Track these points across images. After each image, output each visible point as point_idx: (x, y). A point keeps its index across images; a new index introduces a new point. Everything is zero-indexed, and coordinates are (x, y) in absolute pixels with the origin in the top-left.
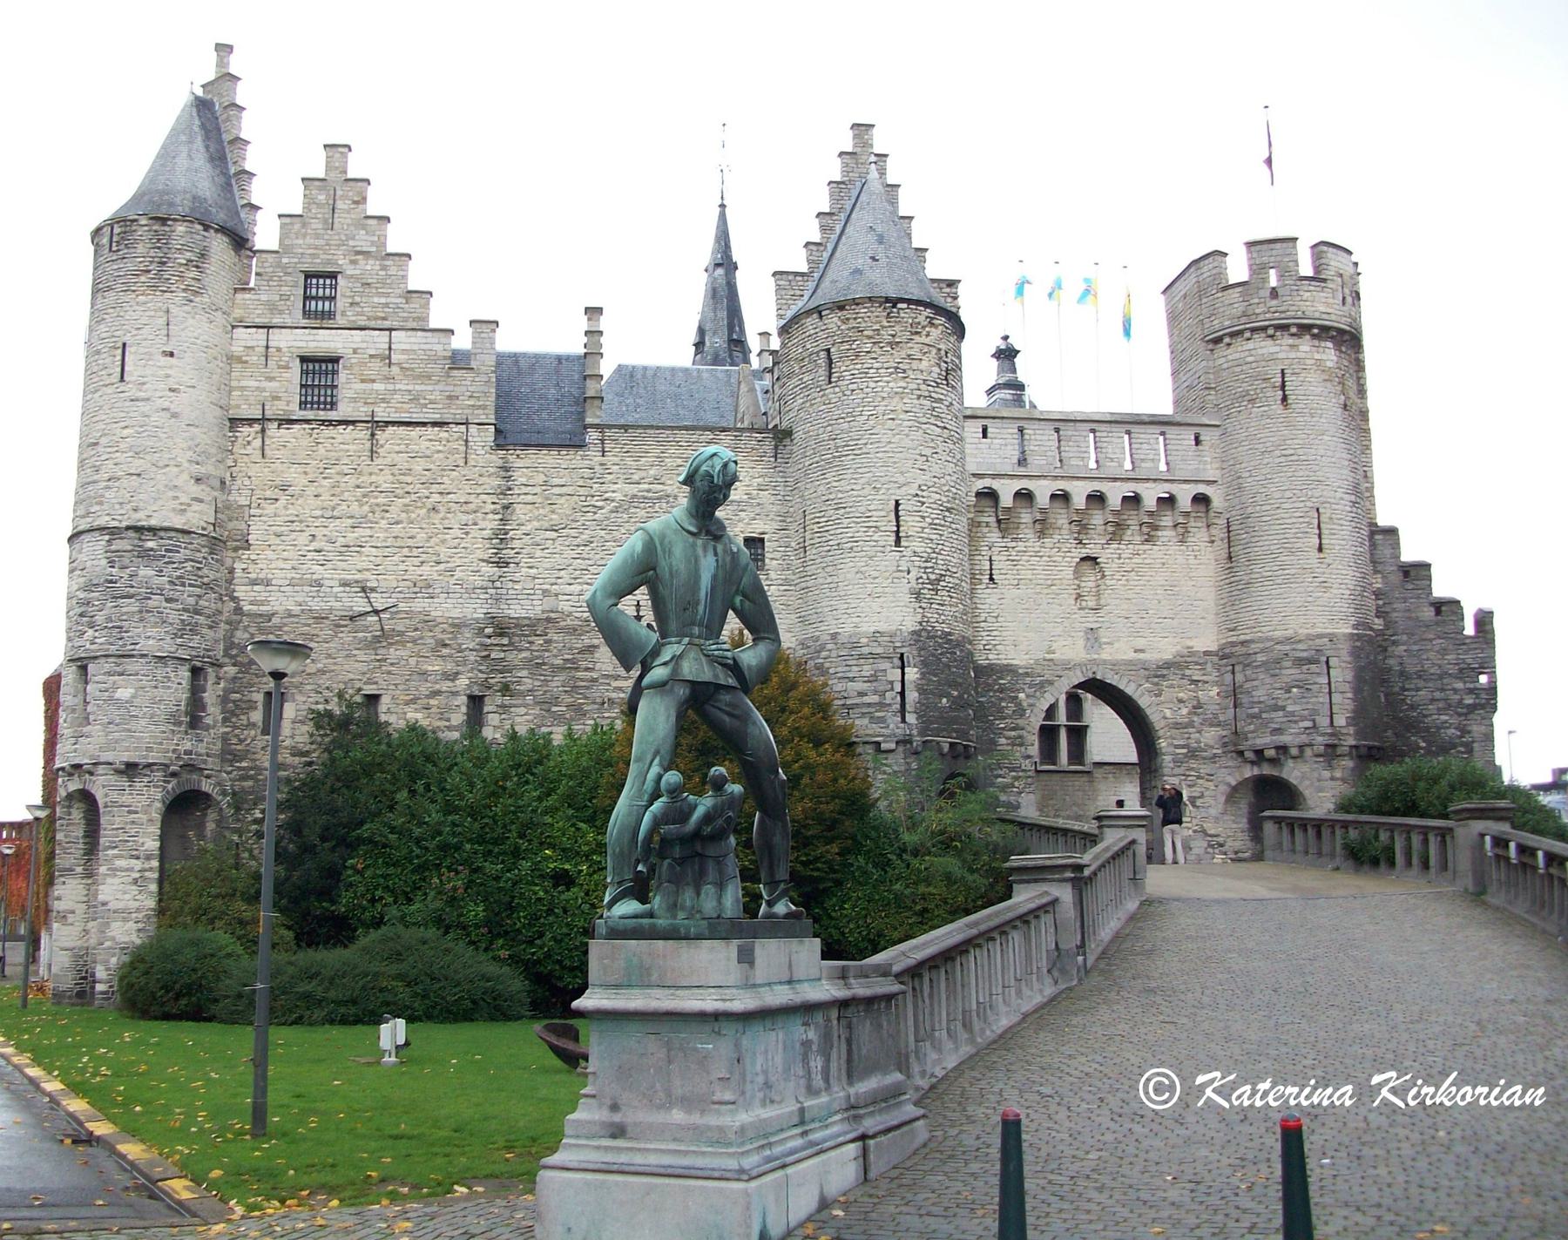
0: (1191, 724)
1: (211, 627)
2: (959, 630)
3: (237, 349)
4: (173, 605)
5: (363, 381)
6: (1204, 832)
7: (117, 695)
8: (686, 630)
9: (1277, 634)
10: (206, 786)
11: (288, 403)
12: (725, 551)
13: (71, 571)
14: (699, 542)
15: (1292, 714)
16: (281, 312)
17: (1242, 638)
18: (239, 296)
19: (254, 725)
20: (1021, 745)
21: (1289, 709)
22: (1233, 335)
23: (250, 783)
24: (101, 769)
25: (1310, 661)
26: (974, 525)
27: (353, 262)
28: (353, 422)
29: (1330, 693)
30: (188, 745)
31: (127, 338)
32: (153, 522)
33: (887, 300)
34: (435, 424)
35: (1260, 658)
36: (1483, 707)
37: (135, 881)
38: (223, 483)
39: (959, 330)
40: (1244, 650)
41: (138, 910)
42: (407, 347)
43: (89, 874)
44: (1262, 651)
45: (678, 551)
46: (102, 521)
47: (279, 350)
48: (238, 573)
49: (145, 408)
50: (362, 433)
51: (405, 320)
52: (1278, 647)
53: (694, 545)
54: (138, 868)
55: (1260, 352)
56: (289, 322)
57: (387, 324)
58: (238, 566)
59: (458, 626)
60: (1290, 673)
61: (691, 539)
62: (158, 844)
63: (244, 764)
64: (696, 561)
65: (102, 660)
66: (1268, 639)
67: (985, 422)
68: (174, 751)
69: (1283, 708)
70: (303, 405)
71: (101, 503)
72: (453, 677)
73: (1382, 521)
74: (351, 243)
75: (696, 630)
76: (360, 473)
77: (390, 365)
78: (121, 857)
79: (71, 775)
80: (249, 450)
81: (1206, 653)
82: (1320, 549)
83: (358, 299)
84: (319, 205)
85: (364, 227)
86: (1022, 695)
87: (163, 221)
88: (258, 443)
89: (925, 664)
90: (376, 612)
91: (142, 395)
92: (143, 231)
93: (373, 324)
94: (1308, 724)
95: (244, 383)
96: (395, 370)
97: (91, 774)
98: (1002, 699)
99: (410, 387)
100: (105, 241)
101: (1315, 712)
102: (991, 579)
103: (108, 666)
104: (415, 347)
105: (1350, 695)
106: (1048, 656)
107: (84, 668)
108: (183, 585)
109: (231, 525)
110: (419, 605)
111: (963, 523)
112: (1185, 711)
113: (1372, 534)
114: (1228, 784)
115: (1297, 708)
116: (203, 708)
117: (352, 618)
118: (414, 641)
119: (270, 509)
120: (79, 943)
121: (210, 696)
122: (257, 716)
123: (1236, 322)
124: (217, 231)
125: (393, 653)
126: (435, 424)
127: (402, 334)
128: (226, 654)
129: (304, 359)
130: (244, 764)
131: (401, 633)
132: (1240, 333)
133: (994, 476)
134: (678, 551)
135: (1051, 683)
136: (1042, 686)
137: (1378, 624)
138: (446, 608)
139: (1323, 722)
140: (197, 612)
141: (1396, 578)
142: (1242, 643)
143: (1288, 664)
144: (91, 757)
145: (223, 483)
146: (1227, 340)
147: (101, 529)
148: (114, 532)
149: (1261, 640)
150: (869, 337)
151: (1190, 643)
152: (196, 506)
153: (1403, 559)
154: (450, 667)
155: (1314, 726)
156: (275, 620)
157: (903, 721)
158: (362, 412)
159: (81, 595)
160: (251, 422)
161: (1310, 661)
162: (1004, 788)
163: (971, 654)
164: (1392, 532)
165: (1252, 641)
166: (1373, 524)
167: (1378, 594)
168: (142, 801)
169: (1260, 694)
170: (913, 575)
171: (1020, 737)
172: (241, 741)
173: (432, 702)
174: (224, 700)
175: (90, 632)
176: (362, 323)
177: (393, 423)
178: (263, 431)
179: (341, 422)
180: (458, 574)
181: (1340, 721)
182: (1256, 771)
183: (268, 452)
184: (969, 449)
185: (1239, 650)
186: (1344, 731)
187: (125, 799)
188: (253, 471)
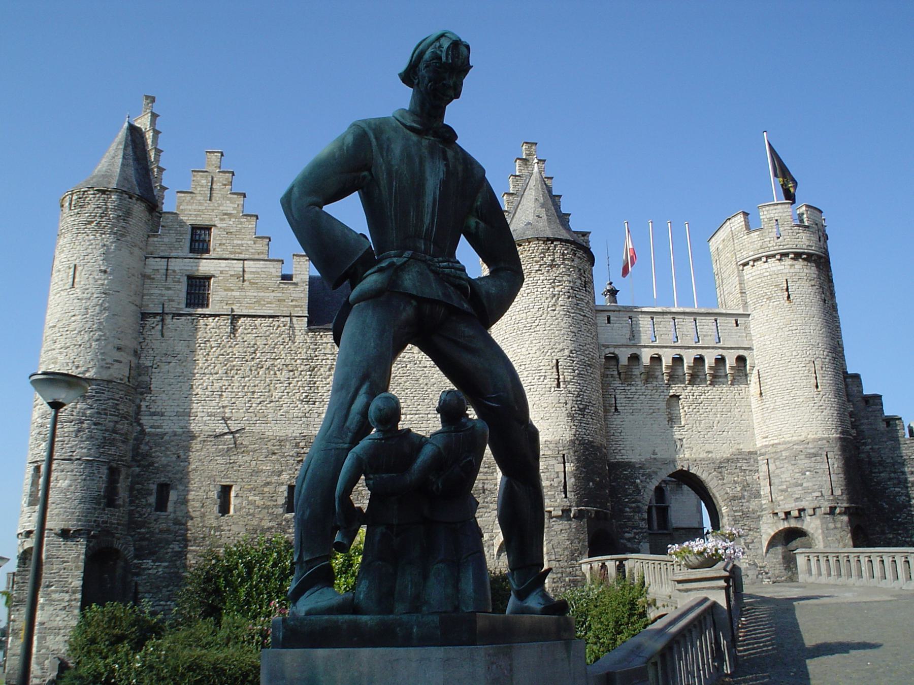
0: (743, 497)
1: (123, 442)
2: (599, 440)
3: (148, 271)
4: (99, 427)
5: (225, 290)
6: (755, 564)
9: (795, 438)
10: (118, 545)
11: (179, 303)
15: (807, 488)
16: (177, 249)
17: (772, 442)
18: (151, 239)
19: (150, 505)
20: (639, 512)
22: (755, 260)
23: (145, 543)
25: (815, 455)
26: (604, 376)
27: (221, 220)
28: (219, 315)
30: (105, 518)
32: (87, 375)
33: (548, 239)
34: (270, 317)
35: (784, 454)
37: (65, 608)
38: (136, 352)
39: (591, 259)
41: (65, 627)
42: (254, 270)
47: (174, 271)
48: (143, 408)
50: (225, 323)
51: (253, 254)
52: (796, 447)
54: (67, 598)
56: (181, 254)
57: (242, 256)
58: (143, 404)
59: (281, 442)
60: (804, 463)
62: (81, 583)
63: (143, 530)
66: (789, 442)
67: (609, 313)
68: (95, 521)
69: (801, 485)
70: (188, 305)
72: (280, 473)
73: (850, 371)
74: (221, 208)
76: (224, 347)
77: (244, 281)
78: (57, 591)
80: (153, 332)
83: (224, 242)
84: (202, 186)
85: (229, 199)
86: (638, 481)
88: (159, 327)
89: (578, 460)
90: (232, 433)
93: (232, 256)
94: (819, 494)
95: (152, 291)
96: (246, 283)
98: (626, 484)
99: (255, 294)
102: (616, 410)
104: (259, 270)
106: (653, 456)
108: (106, 414)
109: (140, 379)
110: (257, 428)
111: (598, 374)
112: (739, 489)
113: (845, 378)
115: (810, 484)
116: (117, 494)
117: (216, 436)
118: (255, 451)
119: (165, 368)
121: (123, 486)
122: (152, 499)
123: (756, 252)
124: (137, 199)
125: (241, 459)
126: (270, 317)
127: (252, 262)
128: (133, 459)
129: (190, 278)
130: (143, 530)
131: (246, 447)
132: (759, 259)
133: (616, 346)
135: (656, 473)
136: (649, 476)
137: (854, 432)
138: (275, 430)
140: (115, 431)
141: (862, 405)
143: (803, 457)
145: (136, 352)
146: (751, 263)
149: (785, 443)
150: (537, 262)
151: (738, 447)
152: (117, 365)
153: (865, 393)
154: (277, 467)
155: (822, 495)
156: (166, 438)
157: (566, 497)
158: (226, 309)
160: (155, 315)
161: (815, 455)
162: (629, 540)
163: (606, 455)
164: (857, 377)
165: (779, 444)
167: (851, 415)
168: (73, 555)
170: (569, 406)
171: (638, 507)
172: (141, 515)
173: (266, 489)
174: (131, 489)
176: (227, 256)
177: (244, 316)
178: (163, 320)
179: (211, 315)
180: (285, 408)
182: (786, 525)
183: (166, 334)
184: (600, 329)
187: (62, 553)
188: (156, 345)
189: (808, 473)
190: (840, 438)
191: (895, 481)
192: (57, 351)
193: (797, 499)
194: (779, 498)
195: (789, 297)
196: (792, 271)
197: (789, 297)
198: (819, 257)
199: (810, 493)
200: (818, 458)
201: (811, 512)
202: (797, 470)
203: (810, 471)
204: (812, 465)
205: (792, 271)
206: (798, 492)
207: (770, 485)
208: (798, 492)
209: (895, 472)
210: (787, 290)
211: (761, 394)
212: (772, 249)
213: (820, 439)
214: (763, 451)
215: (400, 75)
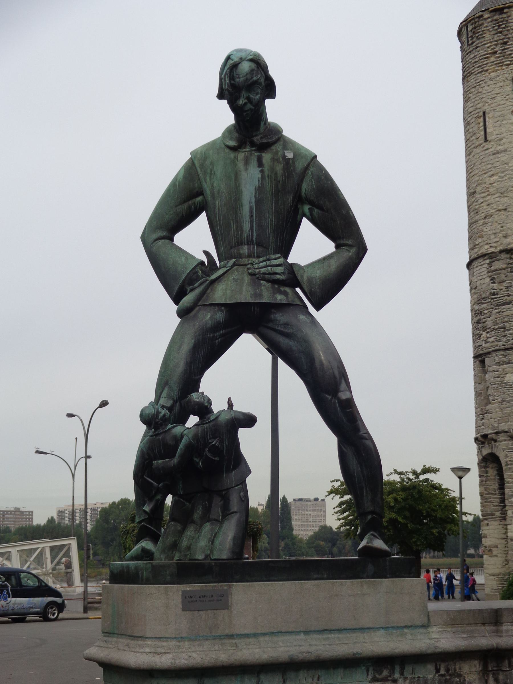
7: (506, 379)
8: (234, 251)
12: (274, 160)
13: (471, 290)
14: (241, 156)
24: (501, 437)
31: (486, 108)
43: (504, 517)
45: (219, 170)
46: (485, 249)
49: (504, 157)
53: (234, 161)
61: (232, 155)
64: (237, 175)
65: (494, 354)
71: (481, 237)
75: (245, 249)
79: (483, 443)
87: (500, 11)
91: (500, 148)
92: (487, 25)
97: (495, 441)
100: (464, 38)
103: (498, 357)
107: (483, 362)
120: (503, 570)
134: (219, 170)
144: (493, 428)
147: (483, 256)
148: (491, 256)
159: (477, 307)
175: (484, 334)
192: (481, 222)
215: (274, 98)
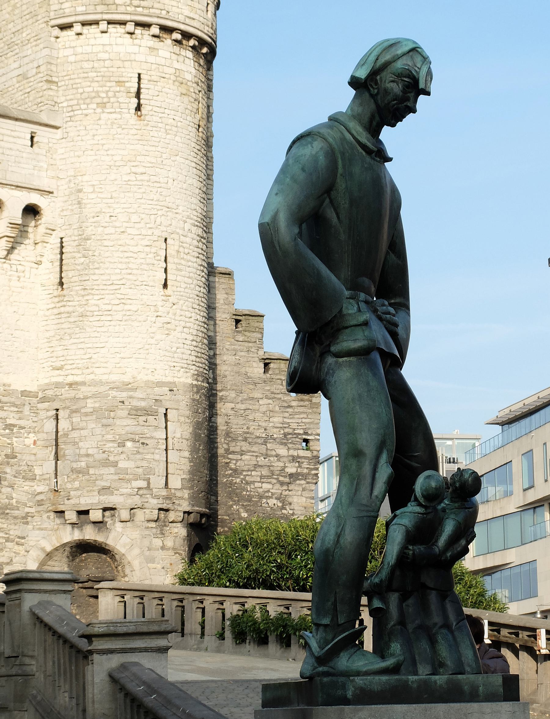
9: (114, 378)
15: (125, 471)
17: (70, 379)
21: (121, 465)
25: (148, 412)
29: (166, 450)
35: (91, 404)
36: (305, 477)
40: (72, 393)
44: (94, 396)
52: (113, 393)
55: (116, 49)
60: (125, 424)
66: (101, 383)
69: (115, 464)
81: (24, 393)
82: (165, 286)
94: (144, 484)
101: (150, 471)
105: (187, 454)
114: (43, 549)
123: (91, 9)
139: (158, 482)
142: (70, 385)
143: (125, 413)
149: (94, 383)
155: (148, 487)
161: (148, 412)
165: (83, 383)
166: (210, 265)
169: (88, 446)
181: (175, 482)
182: (77, 535)
185: (66, 393)
186: (179, 494)
189: (129, 444)
190: (192, 386)
191: (265, 472)
193: (105, 490)
194: (69, 486)
195: (138, 108)
196: (151, 59)
197: (138, 108)
198: (202, 42)
199: (129, 481)
200: (151, 418)
201: (125, 514)
202: (110, 437)
203: (134, 441)
204: (139, 429)
205: (151, 59)
206: (107, 475)
207: (57, 459)
208: (107, 475)
209: (266, 456)
210: (138, 95)
211: (61, 284)
212: (122, 9)
213: (160, 384)
214: (49, 393)
